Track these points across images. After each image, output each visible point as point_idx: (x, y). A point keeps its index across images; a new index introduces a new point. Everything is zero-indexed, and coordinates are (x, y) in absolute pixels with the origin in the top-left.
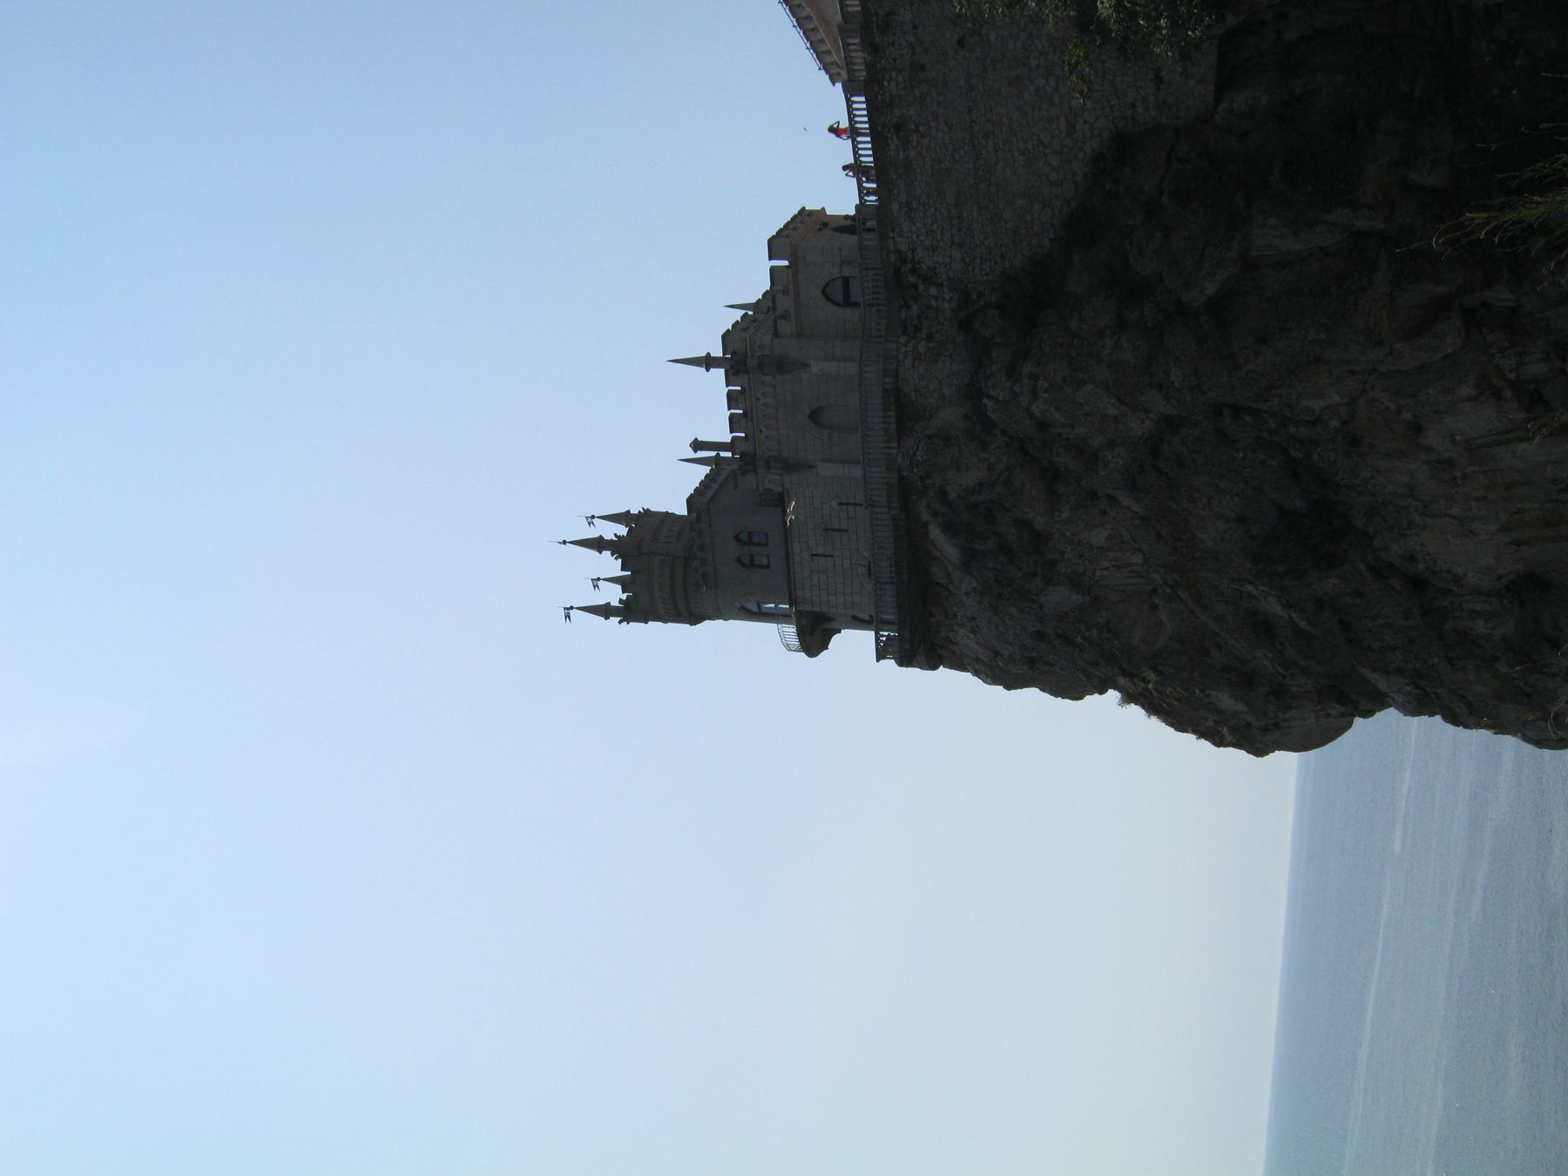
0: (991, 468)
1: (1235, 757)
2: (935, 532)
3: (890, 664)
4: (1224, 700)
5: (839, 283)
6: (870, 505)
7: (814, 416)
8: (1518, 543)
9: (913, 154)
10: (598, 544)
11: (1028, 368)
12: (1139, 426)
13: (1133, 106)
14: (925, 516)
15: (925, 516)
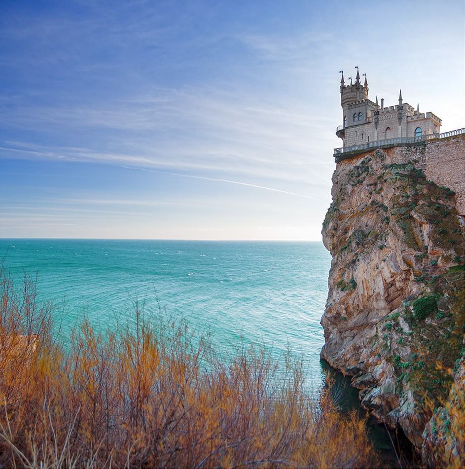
0: (377, 170)
1: (321, 227)
2: (363, 159)
3: (333, 152)
4: (331, 224)
5: (421, 131)
6: (368, 144)
7: (388, 128)
8: (363, 282)
9: (451, 146)
10: (358, 78)
11: (398, 177)
12: (386, 203)
13: (461, 197)
14: (366, 157)
15: (366, 157)
